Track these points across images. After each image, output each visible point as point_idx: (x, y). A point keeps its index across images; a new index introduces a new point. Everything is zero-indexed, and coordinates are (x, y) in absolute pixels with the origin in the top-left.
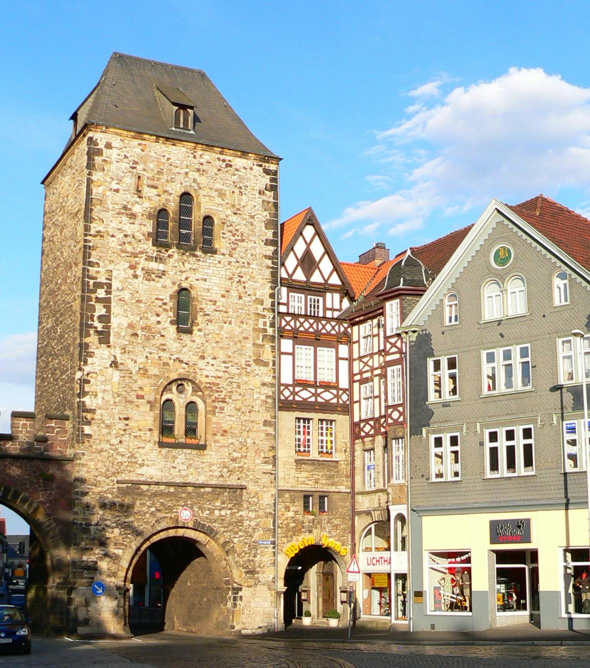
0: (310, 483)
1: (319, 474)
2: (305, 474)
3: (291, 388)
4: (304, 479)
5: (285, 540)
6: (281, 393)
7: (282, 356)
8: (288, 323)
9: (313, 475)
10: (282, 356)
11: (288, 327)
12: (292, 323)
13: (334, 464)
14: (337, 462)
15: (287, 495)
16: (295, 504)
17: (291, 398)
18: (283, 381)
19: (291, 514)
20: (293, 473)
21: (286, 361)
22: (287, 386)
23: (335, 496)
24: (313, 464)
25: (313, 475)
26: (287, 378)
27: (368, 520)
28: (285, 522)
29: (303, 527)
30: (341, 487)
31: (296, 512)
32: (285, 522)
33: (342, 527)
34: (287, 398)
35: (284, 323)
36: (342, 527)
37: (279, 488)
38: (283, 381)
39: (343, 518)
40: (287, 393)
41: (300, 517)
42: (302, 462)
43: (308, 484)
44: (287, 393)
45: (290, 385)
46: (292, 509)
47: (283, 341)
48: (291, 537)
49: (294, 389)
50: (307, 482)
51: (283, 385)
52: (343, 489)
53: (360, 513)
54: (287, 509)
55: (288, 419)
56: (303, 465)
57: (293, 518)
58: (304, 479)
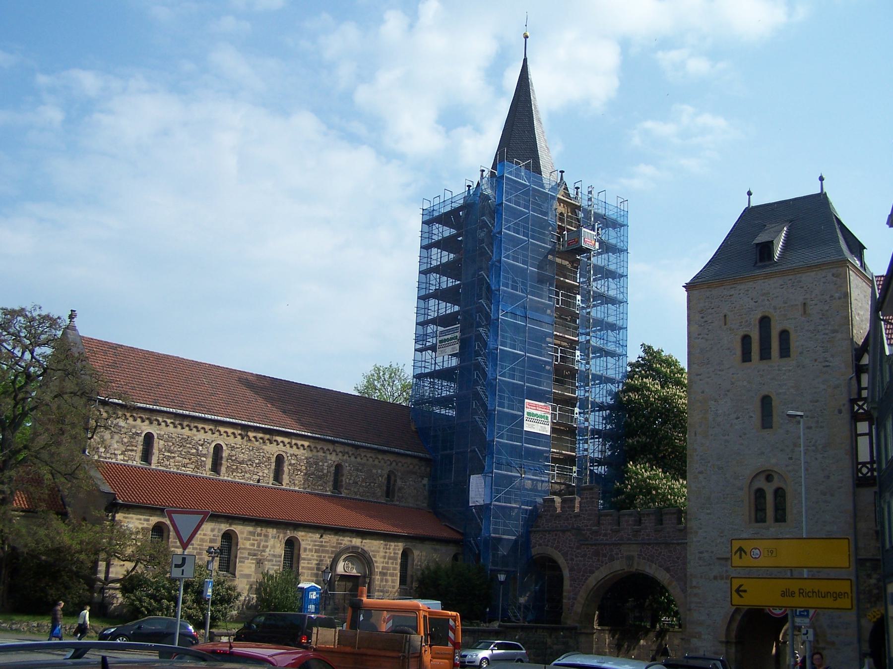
3: (869, 466)
5: (869, 605)
6: (860, 470)
7: (859, 438)
8: (861, 407)
10: (859, 438)
11: (861, 411)
12: (865, 407)
15: (868, 564)
17: (869, 474)
18: (860, 461)
19: (873, 581)
21: (863, 444)
22: (864, 464)
26: (864, 455)
34: (865, 475)
35: (856, 408)
38: (860, 461)
40: (865, 470)
44: (865, 470)
45: (868, 463)
47: (859, 424)
49: (872, 466)
51: (860, 463)
54: (869, 576)
55: (867, 495)
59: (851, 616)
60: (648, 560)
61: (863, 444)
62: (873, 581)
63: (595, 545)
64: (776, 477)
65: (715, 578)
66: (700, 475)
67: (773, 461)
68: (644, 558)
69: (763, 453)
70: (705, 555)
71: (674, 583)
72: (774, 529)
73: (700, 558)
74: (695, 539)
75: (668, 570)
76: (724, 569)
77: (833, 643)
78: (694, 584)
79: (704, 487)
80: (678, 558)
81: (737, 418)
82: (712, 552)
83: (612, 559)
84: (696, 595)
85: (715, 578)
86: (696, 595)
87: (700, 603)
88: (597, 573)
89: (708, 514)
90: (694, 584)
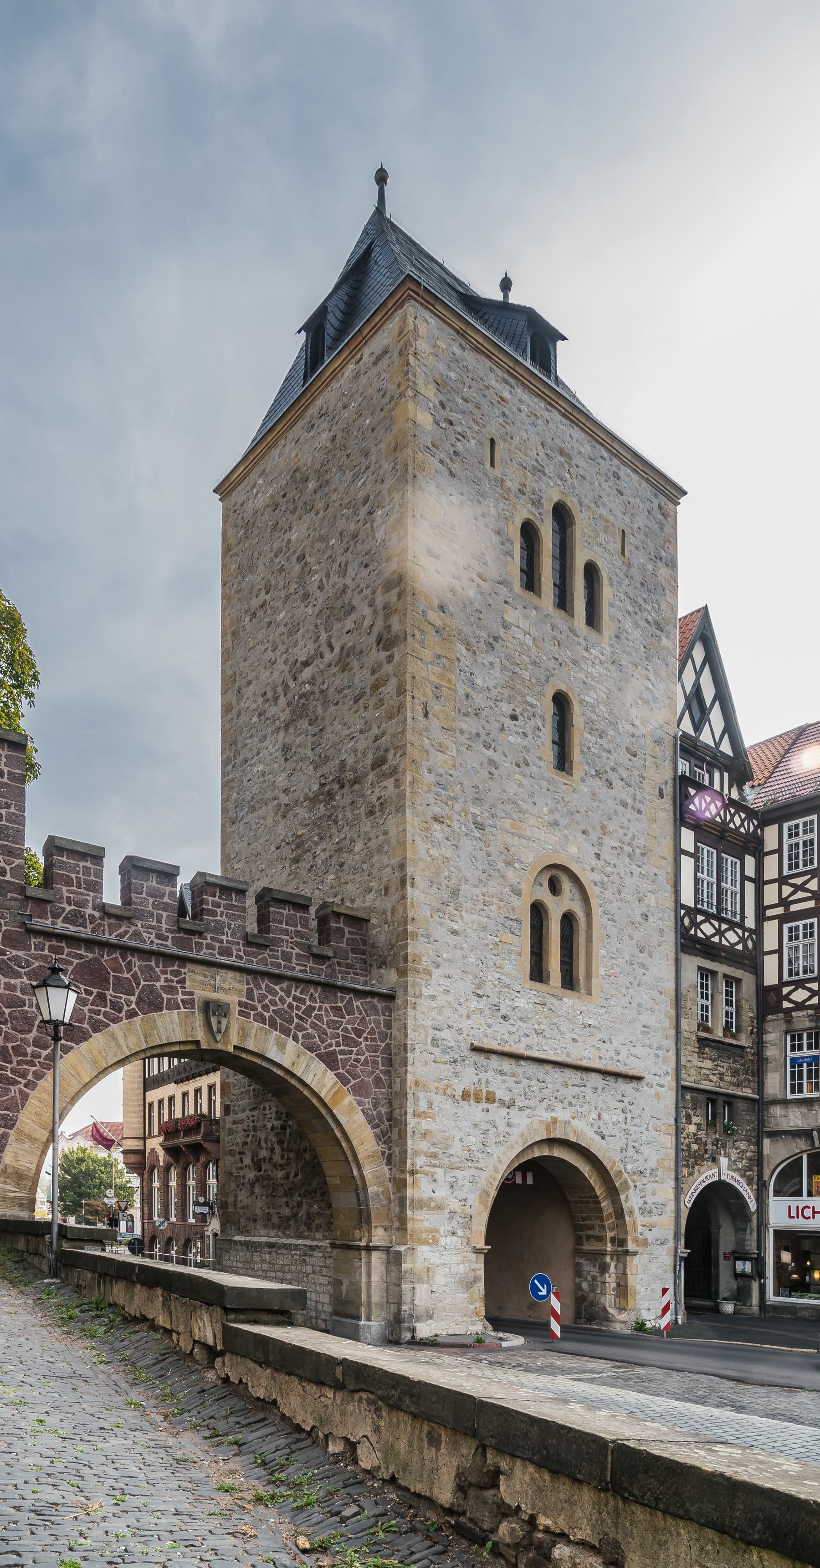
0: (714, 1078)
1: (725, 1066)
2: (708, 1064)
4: (708, 1072)
5: (685, 1171)
9: (717, 1066)
13: (739, 1051)
14: (743, 1048)
16: (698, 1112)
20: (695, 1060)
21: (687, 864)
23: (741, 1105)
24: (718, 1049)
25: (717, 1066)
27: (802, 1144)
28: (687, 1141)
29: (706, 1151)
30: (745, 1090)
31: (698, 1125)
32: (687, 1141)
33: (748, 1154)
36: (748, 1154)
37: (683, 1083)
39: (749, 1141)
41: (702, 1134)
42: (705, 1042)
43: (711, 1081)
46: (695, 1119)
48: (693, 1168)
50: (712, 1077)
52: (748, 1092)
53: (775, 1135)
55: (691, 964)
56: (706, 1049)
57: (695, 1135)
58: (708, 1072)
59: (666, 1191)
60: (273, 1025)
61: (687, 864)
62: (692, 1128)
63: (90, 943)
64: (566, 885)
65: (466, 1096)
66: (437, 826)
67: (573, 850)
68: (262, 1020)
69: (555, 824)
70: (445, 1034)
71: (350, 1098)
72: (570, 1001)
73: (435, 1042)
74: (426, 992)
75: (330, 1060)
76: (482, 1076)
77: (645, 1243)
78: (423, 1106)
79: (446, 860)
80: (359, 1033)
81: (514, 718)
82: (460, 1031)
83: (152, 1003)
84: (424, 1136)
85: (466, 1096)
86: (424, 1136)
87: (435, 1156)
88: (97, 1040)
89: (454, 932)
90: (423, 1106)
